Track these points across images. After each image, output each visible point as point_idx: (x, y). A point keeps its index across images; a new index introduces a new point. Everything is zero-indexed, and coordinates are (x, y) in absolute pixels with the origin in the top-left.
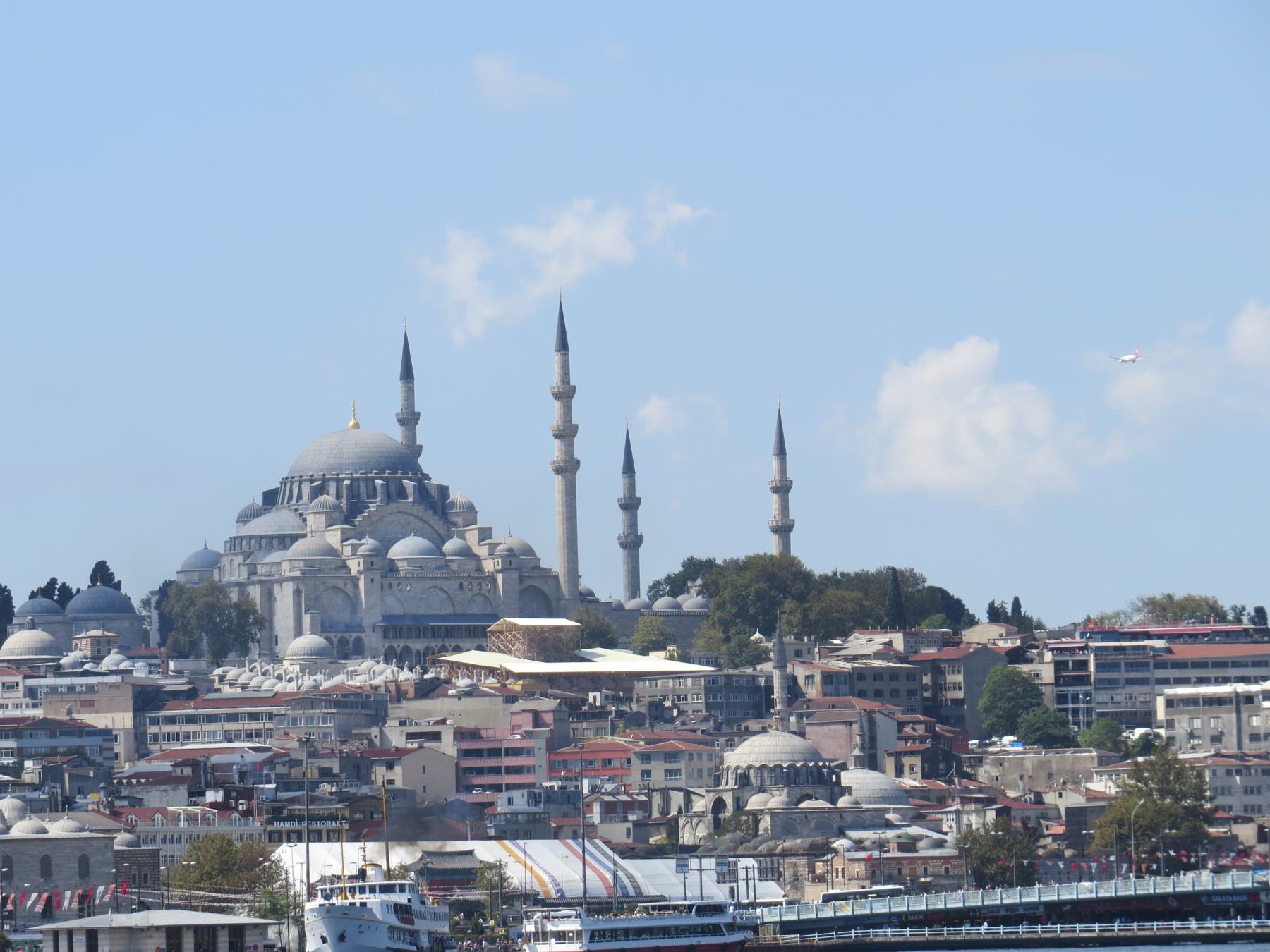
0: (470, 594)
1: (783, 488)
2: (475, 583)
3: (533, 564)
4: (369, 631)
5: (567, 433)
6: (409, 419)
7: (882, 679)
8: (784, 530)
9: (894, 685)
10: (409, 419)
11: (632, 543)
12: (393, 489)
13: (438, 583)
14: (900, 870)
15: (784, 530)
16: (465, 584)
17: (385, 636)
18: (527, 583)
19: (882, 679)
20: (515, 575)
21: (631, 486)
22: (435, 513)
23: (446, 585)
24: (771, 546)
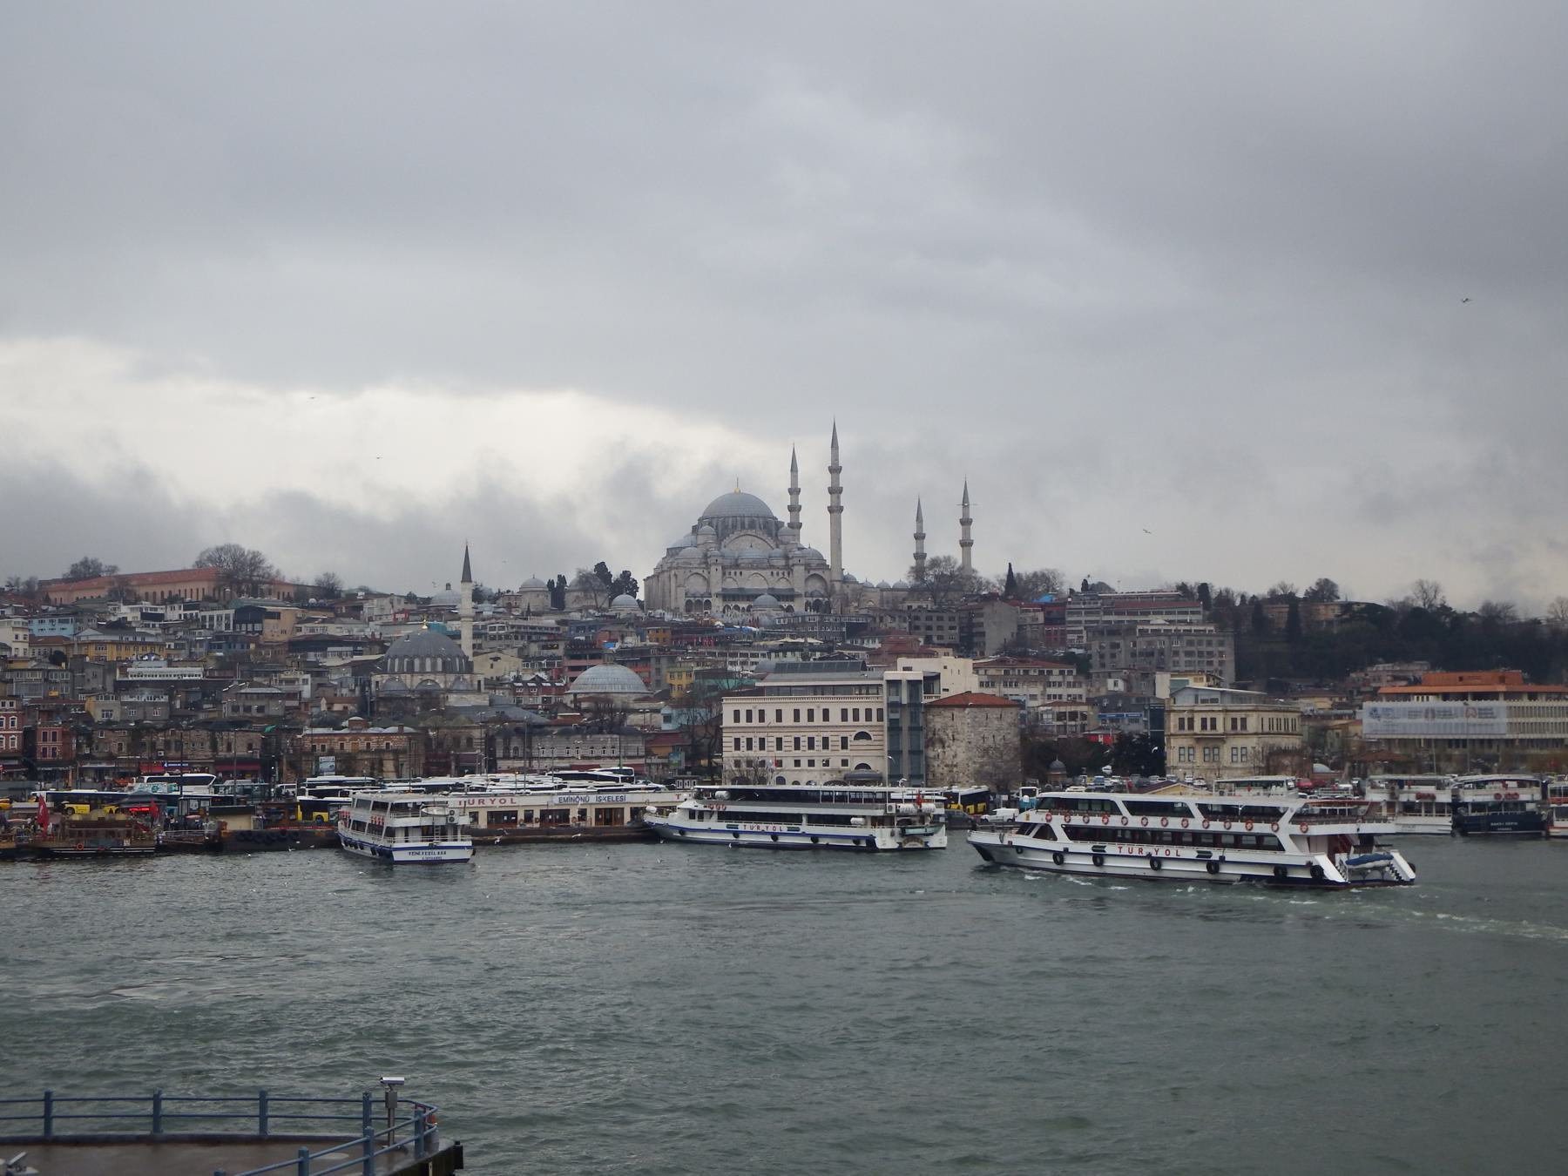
0: (777, 578)
1: (966, 522)
2: (781, 572)
3: (818, 562)
4: (714, 597)
5: (835, 491)
6: (794, 491)
7: (932, 620)
8: (966, 544)
9: (940, 623)
10: (794, 491)
11: (919, 556)
12: (746, 523)
13: (759, 572)
14: (342, 745)
15: (966, 544)
16: (775, 572)
17: (724, 600)
18: (812, 572)
19: (932, 620)
20: (803, 568)
21: (920, 527)
22: (770, 535)
23: (763, 572)
24: (957, 554)
